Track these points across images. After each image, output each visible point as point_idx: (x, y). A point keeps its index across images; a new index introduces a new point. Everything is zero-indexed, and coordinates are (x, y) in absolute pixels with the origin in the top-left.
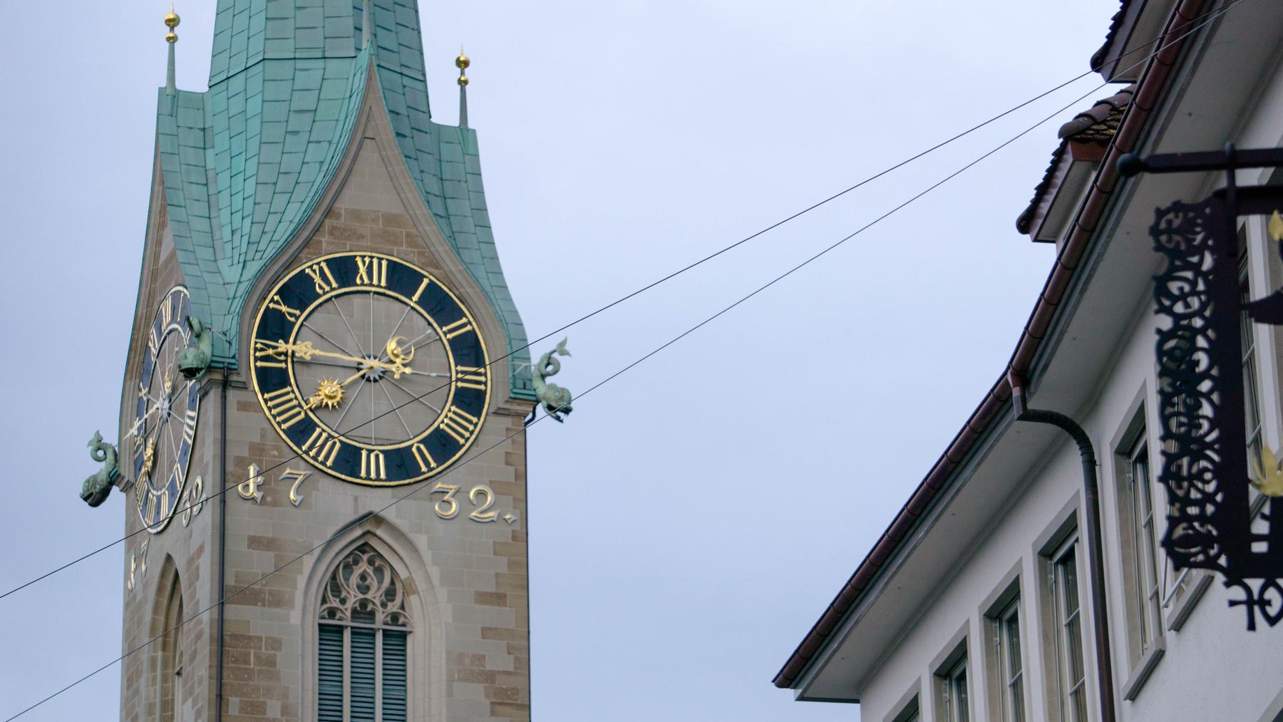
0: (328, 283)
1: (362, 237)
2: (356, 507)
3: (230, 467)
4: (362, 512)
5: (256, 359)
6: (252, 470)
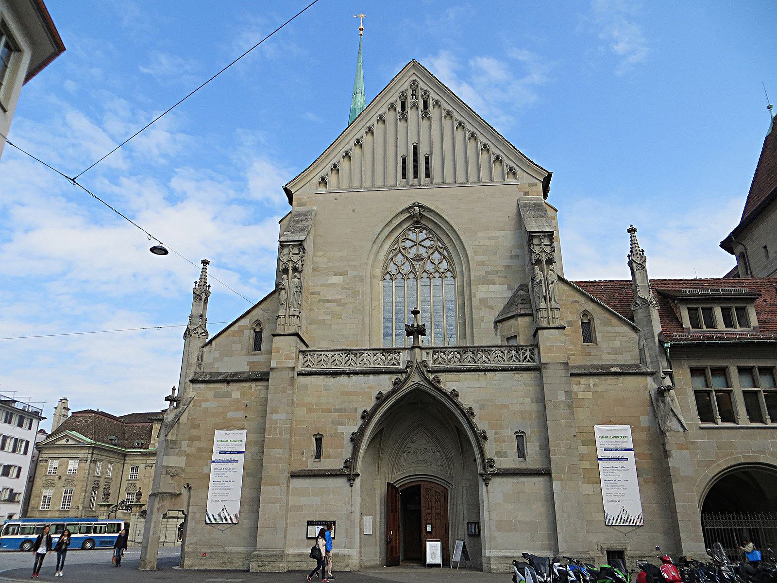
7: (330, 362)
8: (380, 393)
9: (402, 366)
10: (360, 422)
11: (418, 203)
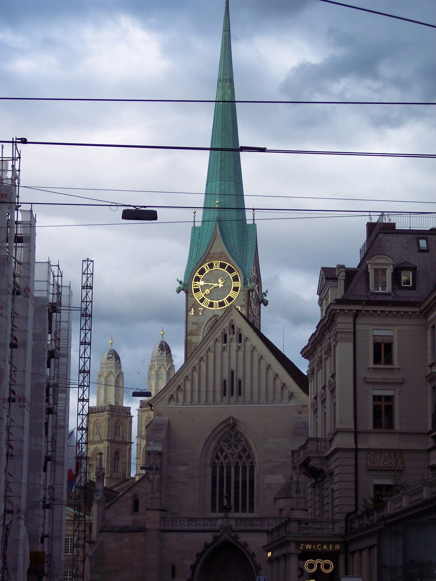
0: (208, 269)
1: (215, 258)
2: (213, 314)
3: (188, 309)
4: (214, 315)
5: (194, 287)
6: (192, 309)
7: (178, 524)
8: (206, 543)
9: (217, 528)
10: (195, 559)
11: (233, 417)
